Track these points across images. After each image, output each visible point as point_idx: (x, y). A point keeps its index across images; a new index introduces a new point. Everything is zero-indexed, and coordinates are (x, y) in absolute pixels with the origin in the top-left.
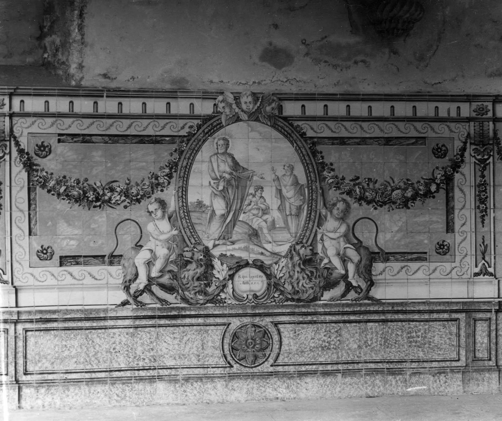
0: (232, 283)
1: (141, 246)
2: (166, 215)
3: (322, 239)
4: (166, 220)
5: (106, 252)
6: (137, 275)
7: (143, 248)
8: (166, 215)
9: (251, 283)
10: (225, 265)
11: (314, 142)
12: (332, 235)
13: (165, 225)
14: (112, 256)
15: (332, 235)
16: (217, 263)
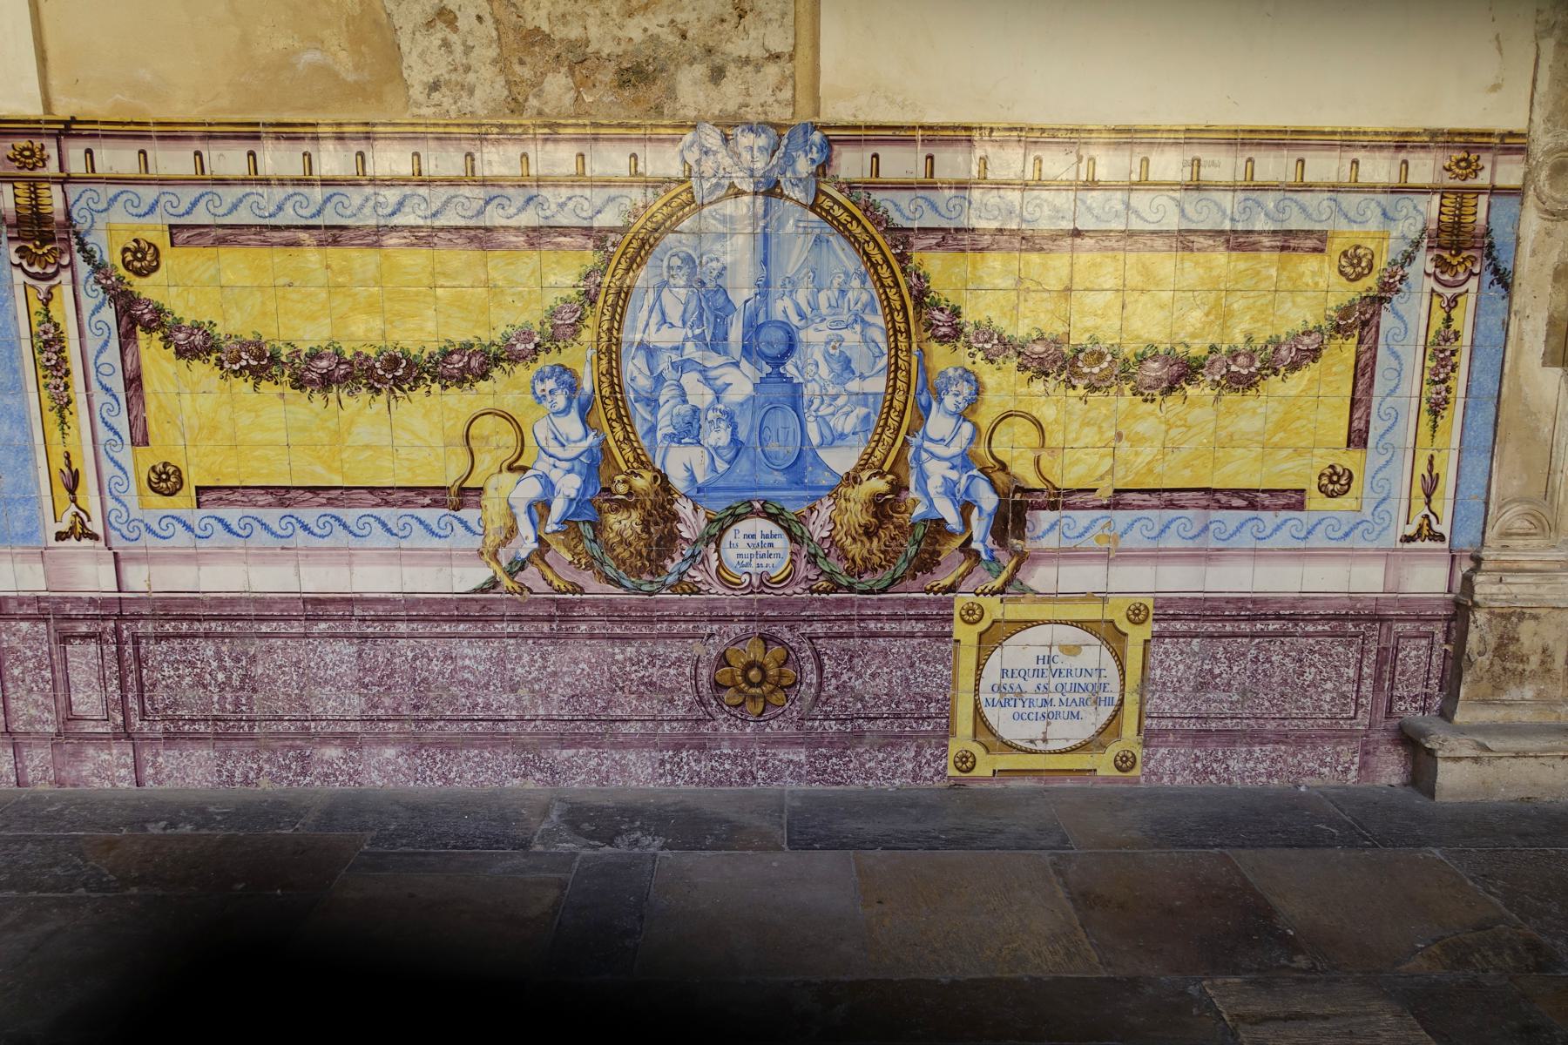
0: (717, 551)
1: (524, 469)
2: (575, 404)
3: (917, 458)
4: (574, 414)
5: (450, 478)
6: (513, 531)
7: (529, 473)
8: (575, 404)
9: (754, 549)
10: (702, 513)
11: (902, 237)
12: (939, 450)
13: (571, 425)
14: (462, 491)
15: (939, 450)
16: (684, 508)
